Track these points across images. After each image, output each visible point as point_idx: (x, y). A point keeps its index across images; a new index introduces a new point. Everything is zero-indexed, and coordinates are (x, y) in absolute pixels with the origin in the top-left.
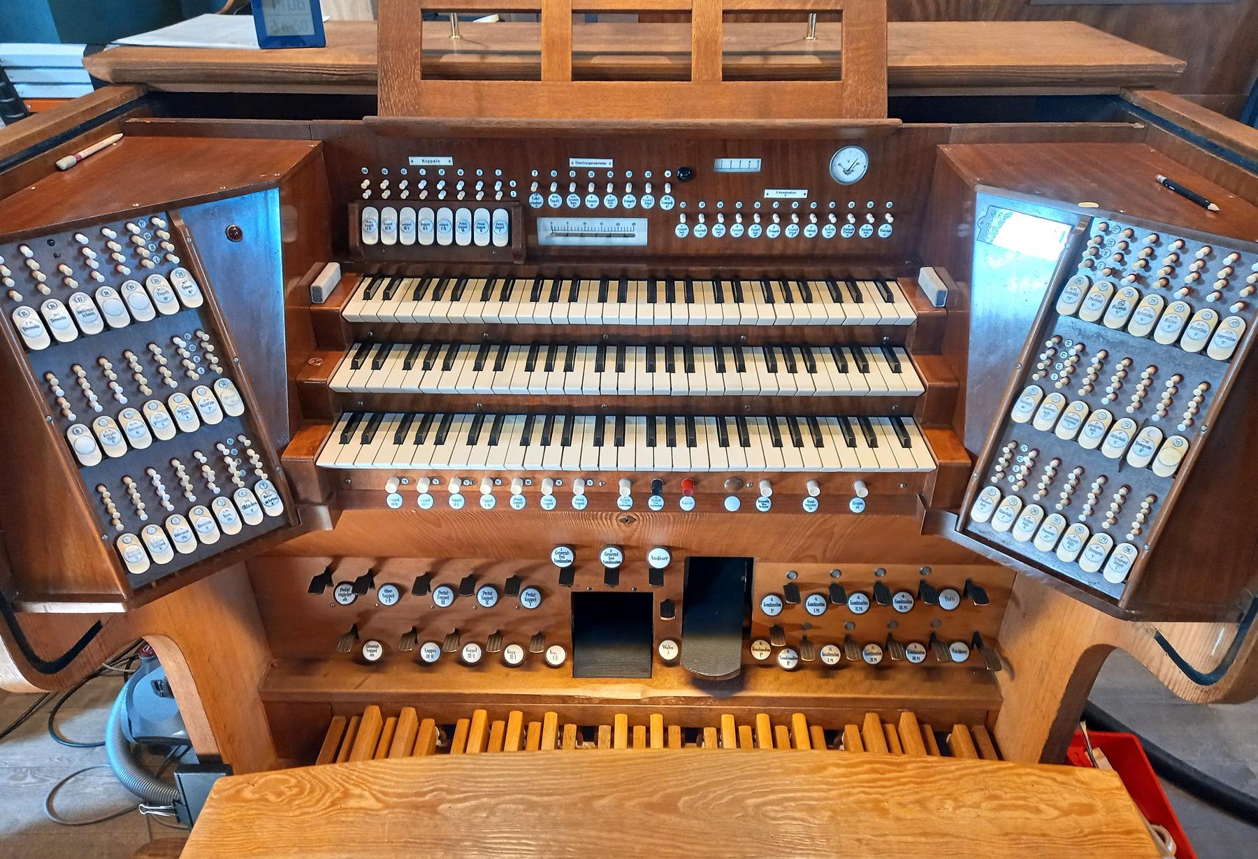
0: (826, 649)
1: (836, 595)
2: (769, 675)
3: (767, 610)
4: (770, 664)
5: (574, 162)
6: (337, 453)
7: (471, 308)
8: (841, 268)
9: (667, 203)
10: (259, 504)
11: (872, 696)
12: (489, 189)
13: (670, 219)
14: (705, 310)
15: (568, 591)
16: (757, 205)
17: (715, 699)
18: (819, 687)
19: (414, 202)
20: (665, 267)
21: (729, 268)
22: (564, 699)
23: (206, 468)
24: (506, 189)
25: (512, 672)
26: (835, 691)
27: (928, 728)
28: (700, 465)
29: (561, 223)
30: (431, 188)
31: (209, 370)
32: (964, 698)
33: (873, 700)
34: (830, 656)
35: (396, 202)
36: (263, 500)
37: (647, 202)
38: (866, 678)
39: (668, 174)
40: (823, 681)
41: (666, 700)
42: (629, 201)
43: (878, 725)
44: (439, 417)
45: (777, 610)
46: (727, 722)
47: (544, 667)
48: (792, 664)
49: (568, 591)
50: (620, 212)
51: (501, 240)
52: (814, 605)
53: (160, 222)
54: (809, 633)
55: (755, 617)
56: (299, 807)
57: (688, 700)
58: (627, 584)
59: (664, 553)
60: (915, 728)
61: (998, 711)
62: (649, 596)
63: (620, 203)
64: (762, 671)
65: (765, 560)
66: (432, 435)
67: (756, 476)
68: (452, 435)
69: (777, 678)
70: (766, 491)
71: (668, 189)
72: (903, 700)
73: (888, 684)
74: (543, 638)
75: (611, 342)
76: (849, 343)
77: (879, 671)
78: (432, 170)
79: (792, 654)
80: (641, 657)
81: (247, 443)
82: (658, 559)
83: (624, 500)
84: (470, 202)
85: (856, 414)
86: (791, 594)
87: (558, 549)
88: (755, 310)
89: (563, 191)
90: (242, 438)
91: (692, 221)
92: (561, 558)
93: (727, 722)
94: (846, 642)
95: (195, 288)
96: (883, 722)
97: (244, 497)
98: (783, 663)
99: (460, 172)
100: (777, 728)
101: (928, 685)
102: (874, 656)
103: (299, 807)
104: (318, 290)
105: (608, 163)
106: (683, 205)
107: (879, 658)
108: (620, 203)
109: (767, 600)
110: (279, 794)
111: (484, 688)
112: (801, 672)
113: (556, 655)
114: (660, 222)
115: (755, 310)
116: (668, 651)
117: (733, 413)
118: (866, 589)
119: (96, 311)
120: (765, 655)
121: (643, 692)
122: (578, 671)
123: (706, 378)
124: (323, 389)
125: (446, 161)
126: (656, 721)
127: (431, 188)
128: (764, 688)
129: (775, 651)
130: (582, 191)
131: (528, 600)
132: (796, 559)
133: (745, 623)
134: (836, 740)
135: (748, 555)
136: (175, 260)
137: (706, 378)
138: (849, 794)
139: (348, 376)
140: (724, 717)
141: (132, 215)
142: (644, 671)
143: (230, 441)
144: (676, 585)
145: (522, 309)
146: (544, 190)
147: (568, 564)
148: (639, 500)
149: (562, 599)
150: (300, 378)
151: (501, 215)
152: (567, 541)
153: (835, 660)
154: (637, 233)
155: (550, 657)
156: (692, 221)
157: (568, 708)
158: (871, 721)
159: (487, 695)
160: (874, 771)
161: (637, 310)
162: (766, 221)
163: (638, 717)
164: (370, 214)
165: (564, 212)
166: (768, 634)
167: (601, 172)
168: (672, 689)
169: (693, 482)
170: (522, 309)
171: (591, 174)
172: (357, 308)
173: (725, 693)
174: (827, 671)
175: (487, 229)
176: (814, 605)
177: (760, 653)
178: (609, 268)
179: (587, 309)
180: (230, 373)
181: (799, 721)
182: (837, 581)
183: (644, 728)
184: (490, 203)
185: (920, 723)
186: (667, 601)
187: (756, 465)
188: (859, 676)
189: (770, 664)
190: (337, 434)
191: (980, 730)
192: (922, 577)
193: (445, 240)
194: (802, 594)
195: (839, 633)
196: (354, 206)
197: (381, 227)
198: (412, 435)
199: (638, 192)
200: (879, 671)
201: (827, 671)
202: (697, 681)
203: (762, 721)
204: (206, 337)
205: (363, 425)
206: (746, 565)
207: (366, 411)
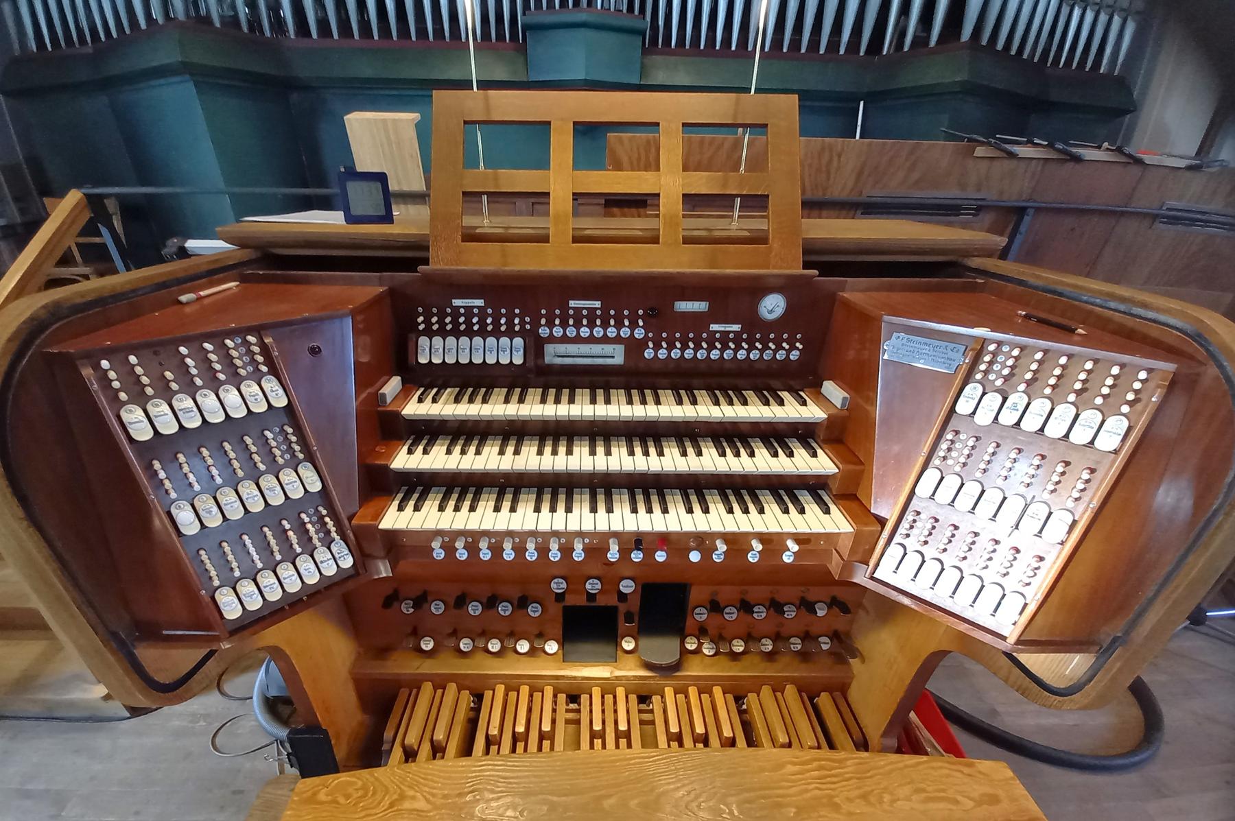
5: (572, 303)
6: (395, 518)
7: (497, 408)
8: (768, 381)
9: (639, 333)
10: (334, 559)
12: (510, 323)
13: (643, 344)
14: (669, 410)
15: (561, 605)
16: (704, 335)
19: (457, 333)
20: (637, 378)
21: (684, 381)
23: (291, 533)
24: (522, 323)
28: (674, 527)
29: (562, 348)
30: (469, 323)
31: (293, 455)
35: (443, 333)
36: (337, 556)
37: (625, 332)
39: (641, 312)
42: (612, 332)
44: (473, 489)
46: (669, 692)
49: (561, 605)
50: (605, 340)
51: (518, 360)
53: (251, 339)
56: (364, 808)
58: (602, 601)
59: (631, 583)
62: (615, 608)
63: (605, 333)
66: (467, 504)
67: (713, 536)
68: (481, 504)
70: (722, 547)
71: (641, 323)
74: (542, 636)
75: (600, 433)
76: (777, 436)
78: (469, 309)
80: (609, 649)
81: (324, 512)
82: (627, 587)
83: (613, 554)
84: (497, 333)
85: (786, 489)
88: (706, 410)
89: (564, 325)
90: (320, 509)
91: (657, 347)
92: (558, 586)
93: (669, 692)
95: (281, 391)
97: (322, 554)
98: (706, 651)
99: (490, 311)
103: (364, 808)
104: (384, 395)
105: (598, 304)
106: (650, 335)
108: (605, 333)
109: (697, 611)
110: (347, 796)
113: (552, 647)
114: (633, 347)
115: (706, 410)
116: (628, 644)
117: (695, 488)
119: (195, 409)
122: (566, 657)
123: (672, 460)
124: (386, 468)
125: (479, 302)
127: (469, 323)
128: (694, 669)
130: (578, 325)
131: (534, 611)
136: (264, 369)
137: (672, 460)
138: (807, 791)
139: (404, 460)
141: (231, 334)
143: (311, 511)
144: (635, 605)
145: (534, 408)
146: (550, 324)
148: (624, 553)
149: (556, 610)
150: (369, 461)
151: (518, 341)
152: (562, 573)
154: (616, 356)
155: (547, 648)
156: (657, 347)
160: (820, 768)
161: (618, 409)
162: (711, 347)
163: (609, 688)
164: (423, 341)
165: (565, 339)
167: (592, 311)
168: (630, 670)
169: (664, 539)
170: (534, 408)
171: (585, 312)
172: (413, 409)
175: (508, 352)
177: (691, 645)
178: (598, 380)
179: (582, 409)
180: (310, 458)
181: (718, 691)
184: (511, 334)
187: (717, 527)
189: (697, 651)
190: (396, 503)
193: (477, 360)
196: (413, 336)
197: (432, 351)
198: (452, 504)
199: (619, 325)
202: (648, 666)
203: (693, 691)
204: (290, 430)
205: (416, 496)
207: (419, 486)
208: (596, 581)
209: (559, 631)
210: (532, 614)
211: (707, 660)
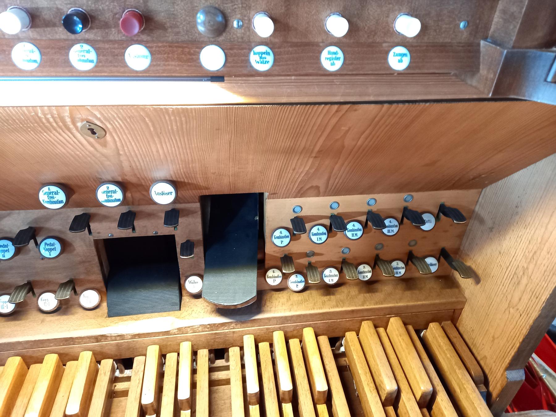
0: (327, 272)
1: (336, 224)
2: (281, 297)
3: (277, 242)
11: (365, 307)
17: (237, 323)
18: (324, 303)
22: (97, 339)
25: (49, 318)
26: (337, 306)
27: (410, 328)
32: (437, 301)
34: (331, 276)
38: (360, 292)
40: (326, 298)
43: (373, 330)
46: (249, 342)
47: (81, 310)
48: (301, 286)
52: (318, 234)
54: (313, 259)
55: (269, 249)
57: (213, 326)
58: (146, 228)
59: (169, 188)
60: (402, 330)
62: (172, 238)
64: (276, 295)
65: (274, 195)
69: (289, 299)
72: (390, 308)
73: (378, 296)
74: (73, 285)
77: (369, 286)
79: (300, 278)
80: (171, 294)
86: (298, 225)
87: (46, 189)
94: (342, 265)
96: (376, 327)
100: (291, 341)
101: (408, 293)
102: (366, 272)
107: (369, 275)
109: (277, 233)
111: (15, 336)
112: (307, 292)
113: (90, 298)
118: (359, 218)
120: (278, 281)
126: (186, 349)
129: (286, 277)
131: (49, 249)
132: (301, 193)
133: (260, 256)
134: (337, 344)
135: (257, 190)
142: (173, 304)
144: (190, 228)
147: (62, 205)
153: (335, 280)
157: (102, 346)
158: (367, 327)
159: (19, 343)
166: (279, 264)
173: (244, 318)
174: (328, 289)
176: (318, 234)
177: (274, 278)
181: (309, 334)
182: (335, 212)
183: (176, 354)
185: (405, 324)
186: (188, 241)
188: (354, 291)
192: (405, 204)
194: (308, 226)
195: (336, 257)
200: (369, 286)
201: (328, 289)
203: (278, 338)
206: (256, 201)
209: (98, 277)
210: (46, 254)
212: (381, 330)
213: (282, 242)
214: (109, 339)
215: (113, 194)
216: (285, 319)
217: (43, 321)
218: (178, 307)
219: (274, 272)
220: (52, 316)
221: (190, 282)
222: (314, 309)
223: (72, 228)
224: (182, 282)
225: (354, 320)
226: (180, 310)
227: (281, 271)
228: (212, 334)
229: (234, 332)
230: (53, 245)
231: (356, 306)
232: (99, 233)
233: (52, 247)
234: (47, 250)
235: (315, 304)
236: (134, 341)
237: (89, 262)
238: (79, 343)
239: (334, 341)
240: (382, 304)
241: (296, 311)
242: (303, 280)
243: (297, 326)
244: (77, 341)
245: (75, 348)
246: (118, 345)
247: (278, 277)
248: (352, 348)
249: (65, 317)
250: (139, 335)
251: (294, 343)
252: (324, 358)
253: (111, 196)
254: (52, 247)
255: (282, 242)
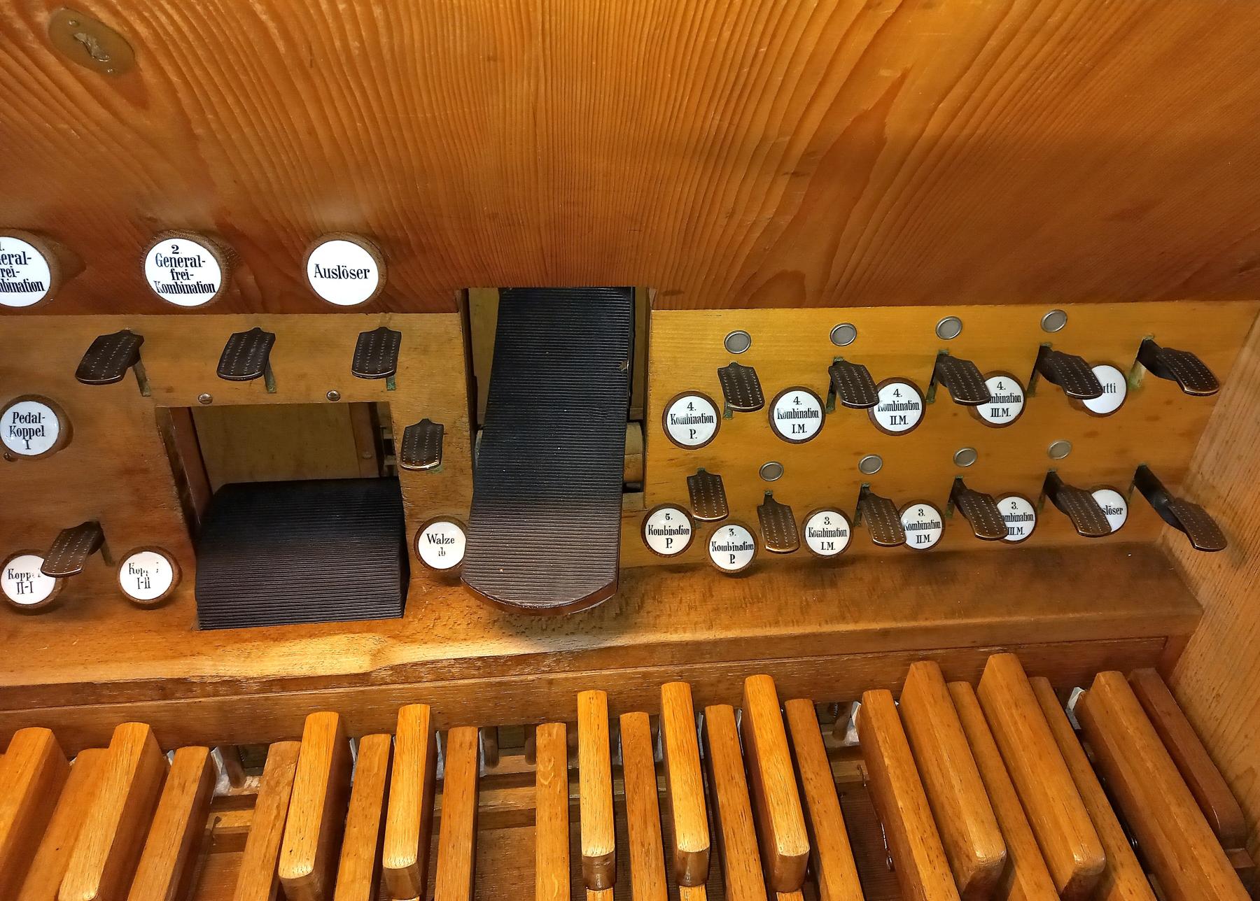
3: (680, 433)
4: (694, 565)
18: (805, 609)
22: (164, 688)
25: (30, 626)
26: (843, 618)
33: (927, 631)
34: (827, 534)
40: (810, 596)
41: (436, 669)
43: (939, 687)
45: (705, 431)
48: (742, 560)
61: (1186, 638)
64: (673, 582)
65: (677, 298)
69: (708, 595)
80: (378, 572)
96: (947, 678)
98: (721, 560)
113: (148, 575)
121: (376, 655)
122: (217, 607)
126: (413, 722)
140: (583, 698)
144: (431, 380)
157: (177, 709)
168: (454, 643)
181: (761, 695)
183: (389, 737)
191: (1148, 674)
203: (675, 700)
208: (189, 248)
211: (727, 591)
212: (963, 688)
213: (692, 432)
214: (198, 690)
215: (191, 270)
216: (694, 651)
217: (12, 635)
218: (396, 608)
219: (668, 517)
220: (42, 622)
221: (432, 539)
222: (777, 623)
223: (83, 373)
224: (410, 538)
225: (890, 661)
226: (402, 616)
227: (688, 515)
228: (491, 685)
229: (551, 682)
230: (37, 419)
231: (895, 620)
232: (170, 390)
233: (35, 426)
234: (20, 433)
235: (779, 610)
236: (267, 699)
237: (145, 471)
238: (113, 700)
239: (831, 714)
240: (967, 614)
241: (727, 628)
242: (750, 541)
243: (729, 669)
244: (106, 692)
245: (104, 711)
246: (221, 707)
247: (680, 531)
248: (880, 736)
249: (78, 625)
250: (284, 683)
251: (720, 717)
252: (802, 762)
253: (185, 275)
254: (35, 426)
255: (692, 432)
